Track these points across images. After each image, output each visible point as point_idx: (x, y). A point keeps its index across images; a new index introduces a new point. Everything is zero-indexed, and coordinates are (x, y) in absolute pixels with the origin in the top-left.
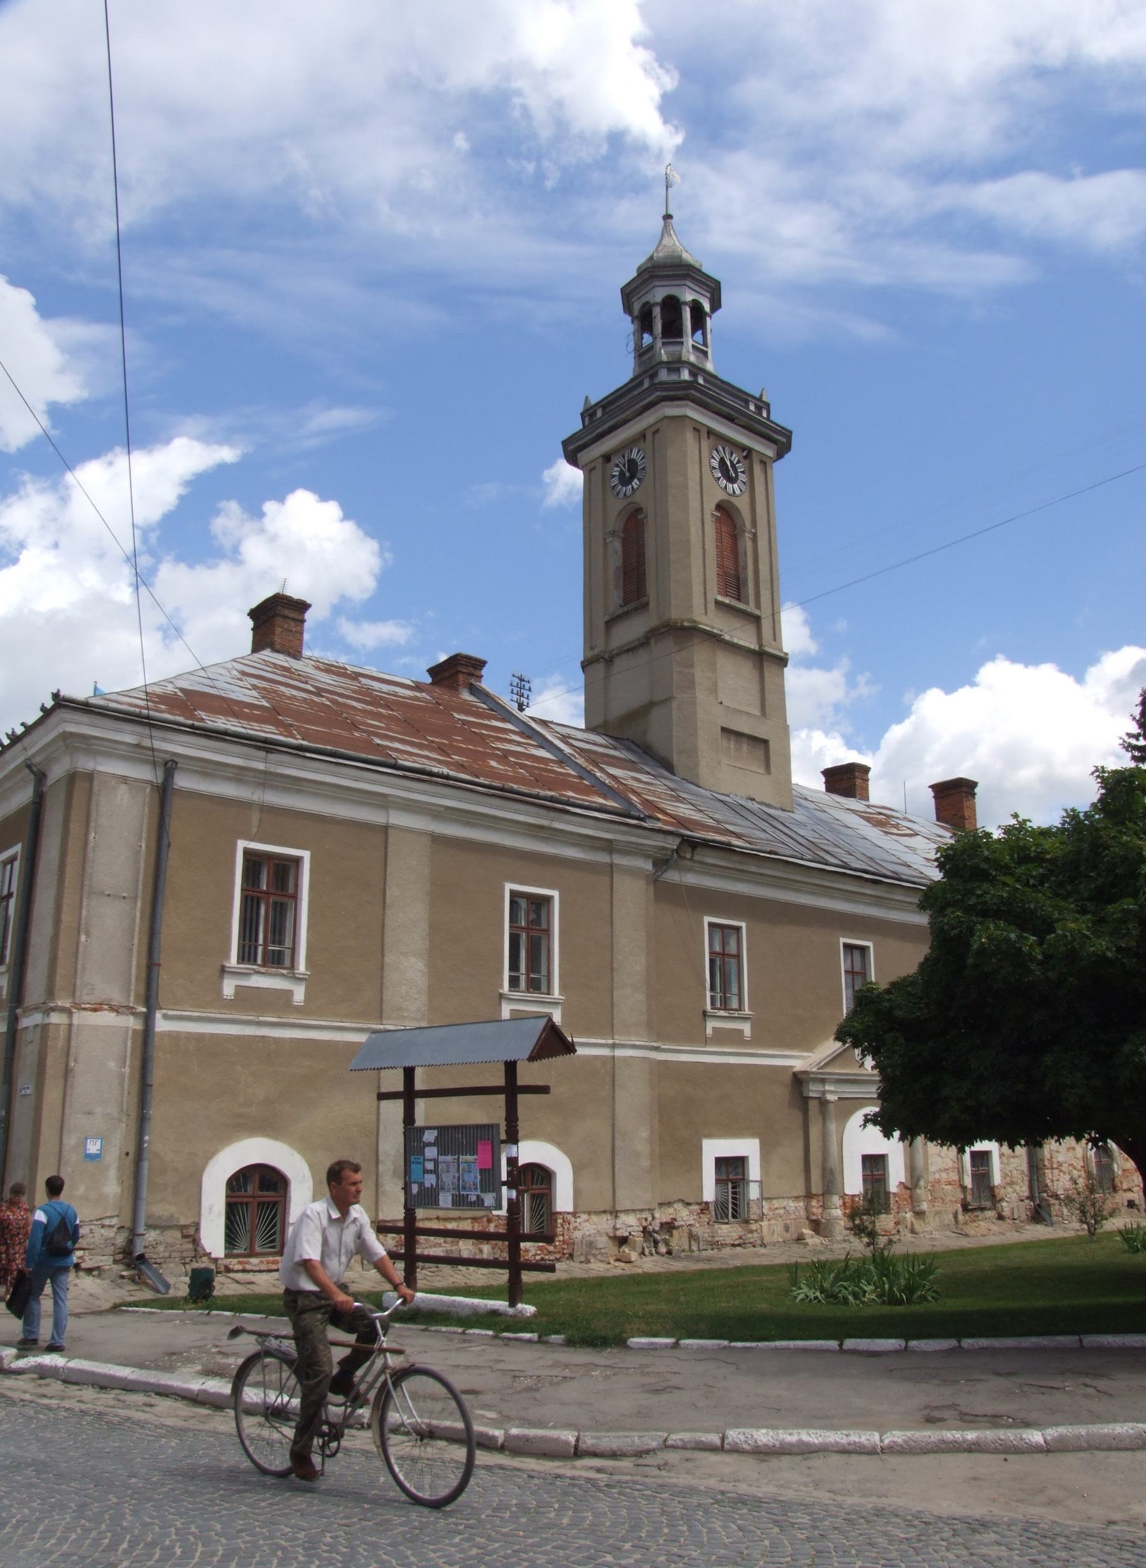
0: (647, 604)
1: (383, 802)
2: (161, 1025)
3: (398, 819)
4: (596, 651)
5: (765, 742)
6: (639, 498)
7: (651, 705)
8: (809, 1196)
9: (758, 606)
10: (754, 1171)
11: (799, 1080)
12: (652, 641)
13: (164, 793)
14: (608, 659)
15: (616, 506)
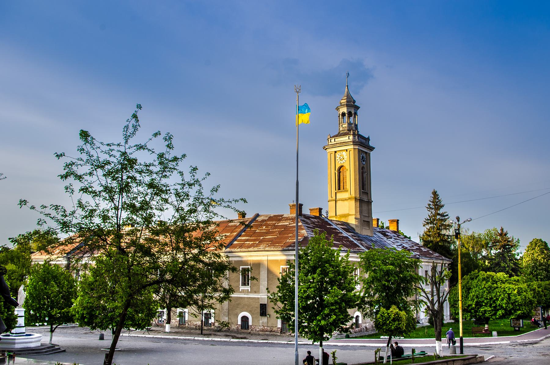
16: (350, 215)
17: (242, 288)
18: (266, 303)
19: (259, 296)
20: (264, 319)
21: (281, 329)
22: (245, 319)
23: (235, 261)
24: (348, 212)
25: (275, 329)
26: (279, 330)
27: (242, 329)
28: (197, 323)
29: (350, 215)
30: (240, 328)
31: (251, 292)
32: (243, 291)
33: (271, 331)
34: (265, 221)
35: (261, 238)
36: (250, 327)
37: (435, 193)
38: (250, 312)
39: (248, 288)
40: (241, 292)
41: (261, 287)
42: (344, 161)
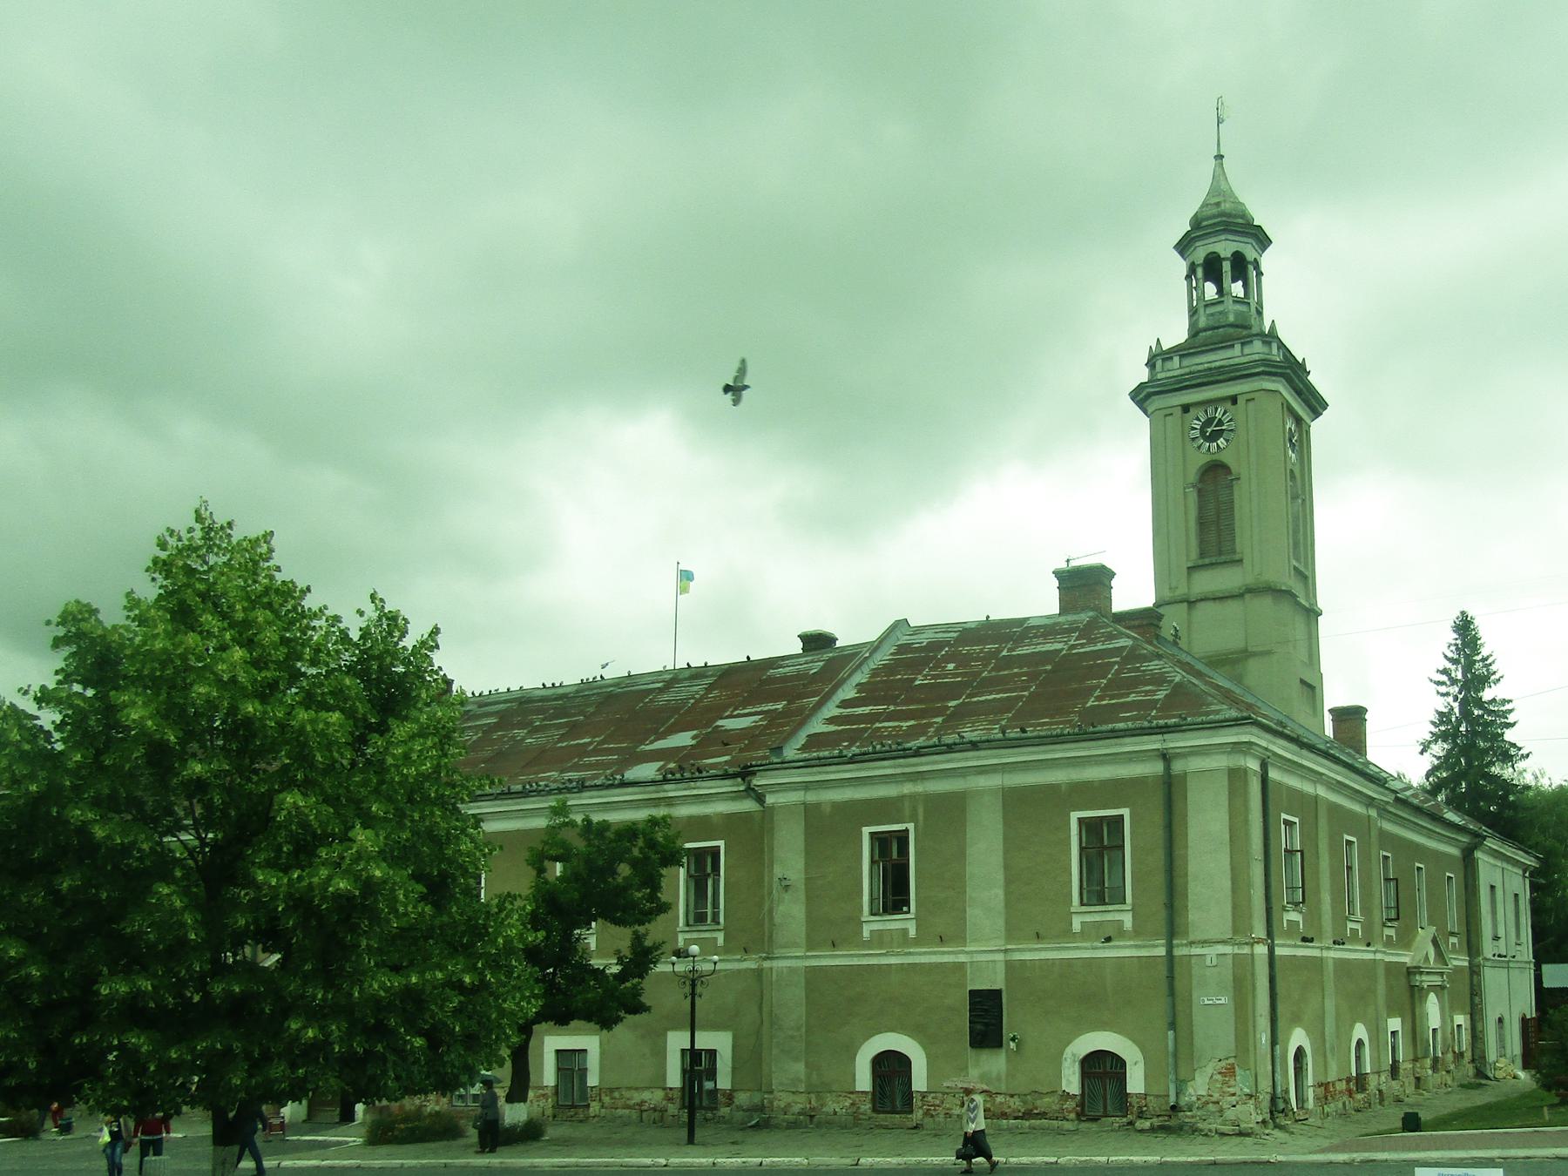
0: (1241, 561)
1: (1317, 777)
2: (1279, 951)
3: (1321, 791)
4: (1178, 593)
5: (1311, 688)
6: (1225, 457)
7: (1246, 654)
8: (1415, 1060)
9: (1306, 565)
10: (593, 1062)
11: (1411, 971)
12: (1247, 596)
13: (1264, 780)
14: (1191, 603)
15: (1199, 460)
16: (1254, 654)
17: (872, 925)
18: (998, 982)
19: (962, 958)
20: (994, 1064)
21: (1082, 1104)
22: (891, 1067)
23: (836, 806)
24: (1241, 645)
25: (1045, 1103)
26: (1070, 1104)
27: (874, 1110)
28: (646, 1095)
29: (1254, 654)
30: (866, 1107)
31: (917, 942)
32: (879, 939)
33: (1028, 1115)
34: (947, 643)
35: (952, 703)
36: (916, 1101)
37: (1464, 627)
38: (916, 1031)
39: (904, 922)
40: (868, 944)
41: (973, 914)
42: (1221, 441)
